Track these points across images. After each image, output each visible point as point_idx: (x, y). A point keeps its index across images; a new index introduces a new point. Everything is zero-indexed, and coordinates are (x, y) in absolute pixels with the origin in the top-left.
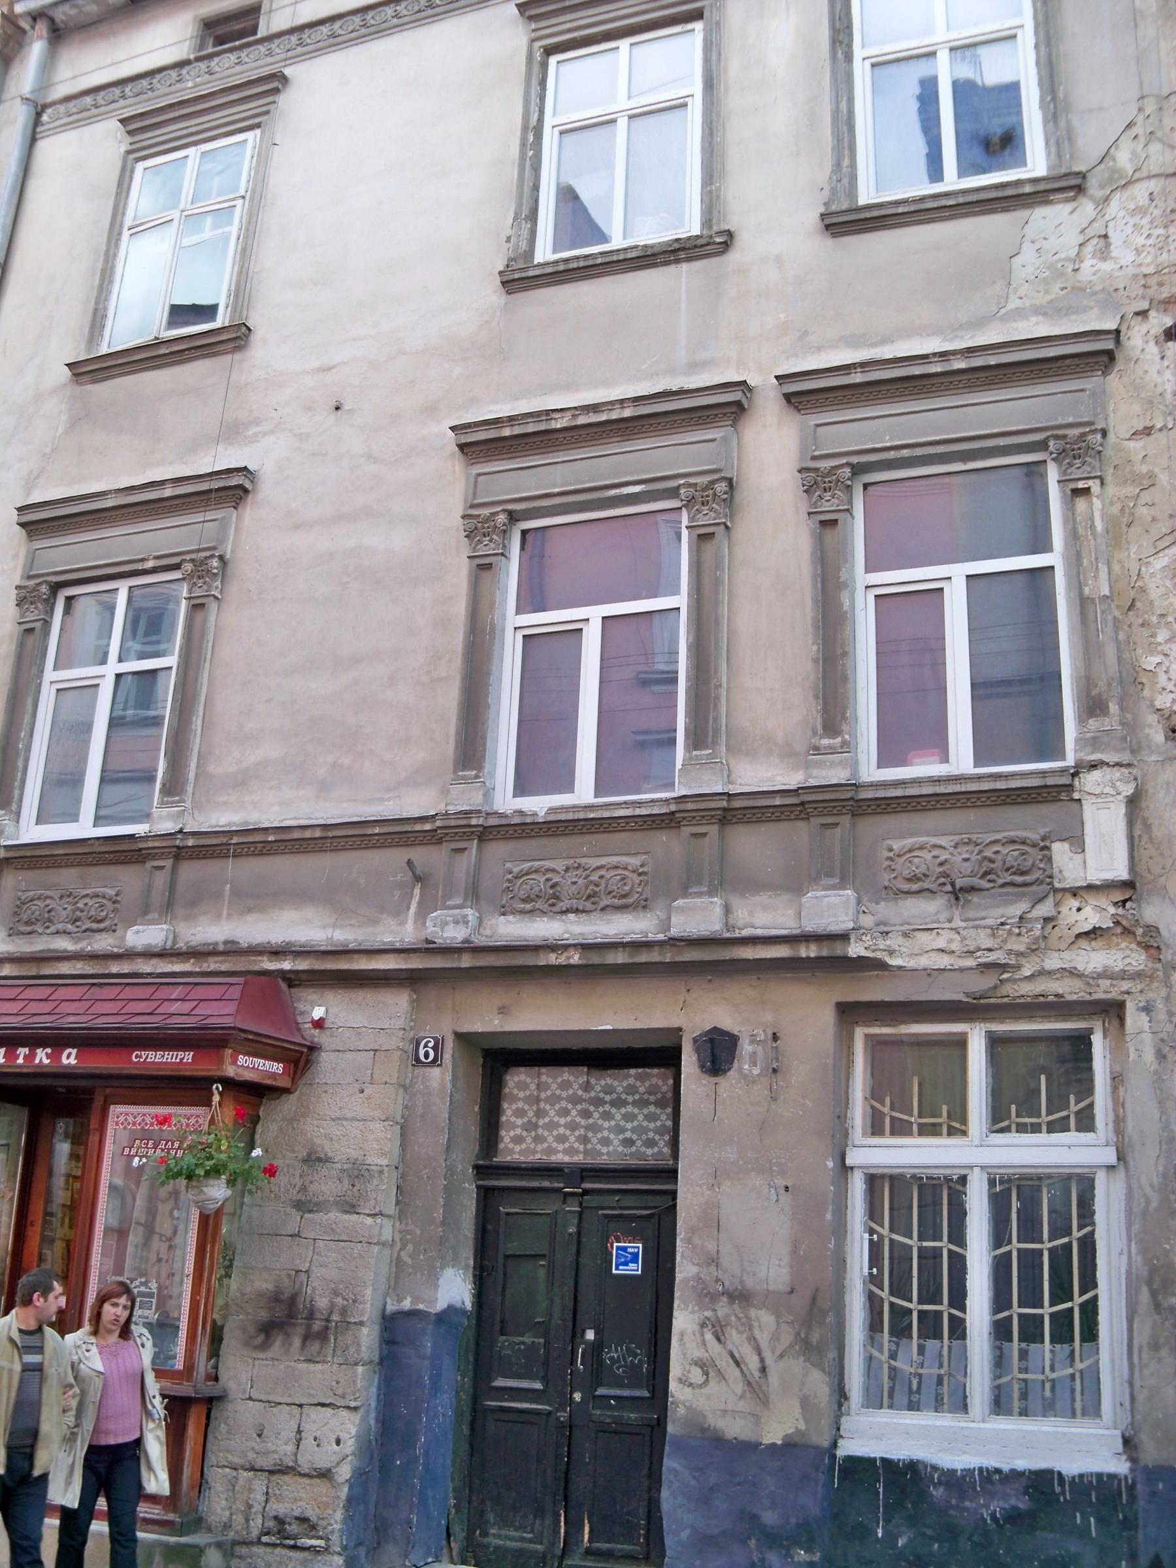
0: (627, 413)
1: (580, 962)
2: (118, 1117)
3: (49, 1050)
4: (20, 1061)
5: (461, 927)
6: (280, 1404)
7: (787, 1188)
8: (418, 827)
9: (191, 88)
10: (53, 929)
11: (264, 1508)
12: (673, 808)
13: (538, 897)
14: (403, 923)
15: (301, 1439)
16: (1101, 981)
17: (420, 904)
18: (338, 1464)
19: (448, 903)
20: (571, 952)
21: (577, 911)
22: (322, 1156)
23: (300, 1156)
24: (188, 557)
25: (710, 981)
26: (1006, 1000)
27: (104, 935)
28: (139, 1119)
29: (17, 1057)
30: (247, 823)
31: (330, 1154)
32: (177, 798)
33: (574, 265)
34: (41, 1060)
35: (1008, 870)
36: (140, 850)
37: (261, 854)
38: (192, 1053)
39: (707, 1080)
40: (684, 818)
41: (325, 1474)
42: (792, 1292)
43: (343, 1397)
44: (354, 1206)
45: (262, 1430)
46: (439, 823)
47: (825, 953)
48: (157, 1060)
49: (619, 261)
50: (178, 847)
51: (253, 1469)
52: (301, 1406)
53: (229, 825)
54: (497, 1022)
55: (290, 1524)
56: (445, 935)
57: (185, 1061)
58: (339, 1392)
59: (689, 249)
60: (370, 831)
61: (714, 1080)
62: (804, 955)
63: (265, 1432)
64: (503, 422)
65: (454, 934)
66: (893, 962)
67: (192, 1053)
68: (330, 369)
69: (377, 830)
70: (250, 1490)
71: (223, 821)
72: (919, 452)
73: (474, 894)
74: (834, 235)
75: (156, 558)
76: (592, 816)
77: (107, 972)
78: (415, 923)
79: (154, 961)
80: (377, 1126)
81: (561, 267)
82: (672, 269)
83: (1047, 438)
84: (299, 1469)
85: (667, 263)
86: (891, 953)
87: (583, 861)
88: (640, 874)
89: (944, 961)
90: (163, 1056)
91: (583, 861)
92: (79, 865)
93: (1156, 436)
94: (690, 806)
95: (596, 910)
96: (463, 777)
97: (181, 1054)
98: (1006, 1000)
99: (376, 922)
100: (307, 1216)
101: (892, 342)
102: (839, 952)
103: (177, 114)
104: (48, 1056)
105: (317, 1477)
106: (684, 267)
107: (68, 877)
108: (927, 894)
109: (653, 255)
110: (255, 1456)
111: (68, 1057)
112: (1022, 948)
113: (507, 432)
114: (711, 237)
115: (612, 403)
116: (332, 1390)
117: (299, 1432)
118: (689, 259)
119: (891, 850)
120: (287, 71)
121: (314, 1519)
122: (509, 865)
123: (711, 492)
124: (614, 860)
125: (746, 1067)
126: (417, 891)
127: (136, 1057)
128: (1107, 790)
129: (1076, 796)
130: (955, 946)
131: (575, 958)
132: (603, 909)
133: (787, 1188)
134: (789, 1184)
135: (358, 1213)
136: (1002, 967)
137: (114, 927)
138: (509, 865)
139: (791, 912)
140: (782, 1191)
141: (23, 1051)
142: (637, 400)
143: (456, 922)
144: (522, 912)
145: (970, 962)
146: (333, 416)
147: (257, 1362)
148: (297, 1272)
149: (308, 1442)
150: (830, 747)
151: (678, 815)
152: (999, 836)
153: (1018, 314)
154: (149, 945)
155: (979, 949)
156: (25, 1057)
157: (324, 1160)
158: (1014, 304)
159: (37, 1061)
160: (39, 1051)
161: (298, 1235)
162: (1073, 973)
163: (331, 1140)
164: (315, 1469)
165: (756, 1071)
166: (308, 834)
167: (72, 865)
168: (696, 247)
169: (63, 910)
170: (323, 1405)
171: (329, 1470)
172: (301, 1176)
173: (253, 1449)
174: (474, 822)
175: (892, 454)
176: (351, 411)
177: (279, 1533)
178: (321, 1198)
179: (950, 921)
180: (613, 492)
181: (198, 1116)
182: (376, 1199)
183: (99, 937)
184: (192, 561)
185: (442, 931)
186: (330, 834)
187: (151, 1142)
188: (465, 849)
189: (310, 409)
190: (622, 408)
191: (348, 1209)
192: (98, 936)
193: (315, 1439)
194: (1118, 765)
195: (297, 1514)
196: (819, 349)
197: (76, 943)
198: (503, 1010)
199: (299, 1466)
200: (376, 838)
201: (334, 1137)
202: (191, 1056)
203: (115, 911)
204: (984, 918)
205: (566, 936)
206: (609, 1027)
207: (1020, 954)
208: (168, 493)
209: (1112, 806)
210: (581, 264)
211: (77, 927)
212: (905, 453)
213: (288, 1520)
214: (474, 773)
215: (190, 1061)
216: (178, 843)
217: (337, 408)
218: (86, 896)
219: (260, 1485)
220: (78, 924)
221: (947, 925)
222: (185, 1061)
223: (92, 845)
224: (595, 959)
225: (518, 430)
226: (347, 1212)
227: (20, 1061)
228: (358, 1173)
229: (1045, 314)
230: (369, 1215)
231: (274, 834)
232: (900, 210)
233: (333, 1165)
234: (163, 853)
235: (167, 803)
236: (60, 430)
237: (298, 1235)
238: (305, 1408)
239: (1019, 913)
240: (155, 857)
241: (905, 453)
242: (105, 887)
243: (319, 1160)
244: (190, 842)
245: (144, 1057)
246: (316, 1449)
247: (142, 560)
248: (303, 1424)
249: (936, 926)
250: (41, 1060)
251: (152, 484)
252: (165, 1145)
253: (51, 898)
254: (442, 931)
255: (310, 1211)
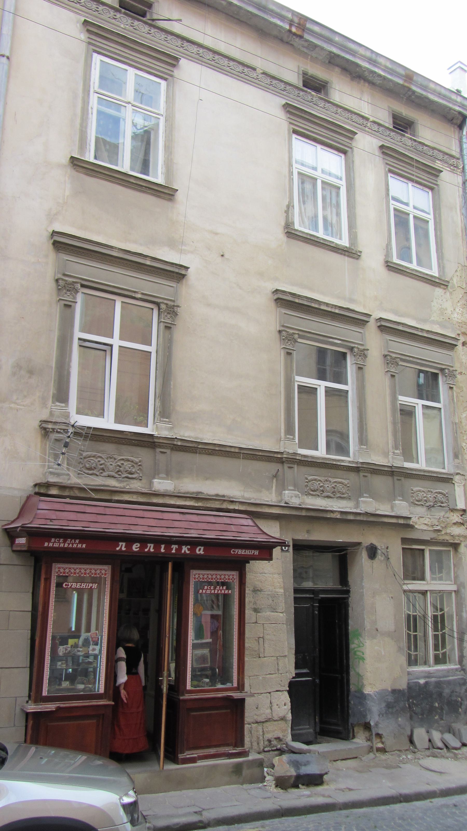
0: (337, 311)
1: (340, 518)
2: (195, 575)
3: (189, 547)
4: (174, 551)
5: (297, 499)
6: (262, 693)
7: (392, 597)
8: (276, 456)
9: (123, 28)
10: (105, 474)
11: (263, 737)
12: (360, 465)
13: (317, 490)
14: (271, 493)
15: (272, 706)
16: (456, 537)
17: (276, 486)
18: (287, 713)
19: (289, 488)
20: (337, 513)
21: (328, 497)
22: (259, 589)
23: (251, 589)
24: (165, 302)
25: (369, 527)
26: (436, 540)
27: (135, 481)
28: (214, 577)
29: (172, 549)
30: (198, 438)
31: (262, 588)
32: (168, 420)
33: (312, 238)
34: (185, 551)
35: (439, 502)
36: (154, 442)
37: (210, 454)
38: (258, 551)
39: (370, 561)
40: (362, 470)
41: (283, 719)
42: (395, 631)
43: (284, 686)
44: (275, 609)
45: (258, 706)
46: (285, 456)
47: (405, 523)
48: (242, 553)
49: (327, 245)
50: (174, 445)
51: (257, 722)
52: (270, 693)
53: (189, 437)
54: (306, 536)
55: (273, 741)
56: (292, 501)
57: (255, 554)
58: (283, 685)
59: (349, 252)
60: (258, 454)
61: (372, 561)
62: (400, 522)
63: (259, 706)
64: (296, 296)
65: (295, 502)
66: (416, 526)
67: (258, 551)
68: (216, 234)
69: (260, 454)
70: (257, 731)
71: (186, 434)
72: (415, 360)
73: (296, 486)
74: (389, 270)
75: (143, 294)
76: (334, 463)
77: (151, 501)
78: (276, 494)
79: (176, 498)
80: (276, 576)
81: (309, 237)
82: (342, 257)
83: (446, 368)
84: (274, 719)
85: (341, 254)
86: (416, 523)
87: (330, 479)
88: (348, 487)
89: (425, 528)
90: (245, 552)
91: (330, 479)
92: (116, 443)
93: (463, 375)
94: (365, 466)
95: (335, 497)
96: (288, 438)
97: (253, 551)
98: (436, 540)
99: (261, 492)
100: (258, 614)
101: (404, 317)
102: (408, 523)
103: (120, 41)
104: (188, 549)
105: (280, 720)
106: (346, 258)
107: (110, 448)
108: (421, 506)
109: (339, 249)
110: (257, 717)
111: (200, 550)
112: (443, 526)
113: (297, 301)
114: (356, 251)
115: (333, 305)
116: (280, 684)
117: (271, 703)
118: (348, 256)
119: (413, 490)
120: (183, 62)
121: (281, 737)
122: (306, 476)
123: (363, 353)
124: (340, 480)
125: (380, 557)
126: (275, 481)
127: (233, 551)
128: (460, 482)
129: (453, 482)
130: (429, 524)
131: (339, 516)
132: (337, 498)
133: (392, 597)
134: (392, 596)
135: (277, 612)
136: (439, 531)
137: (141, 478)
138: (306, 476)
139: (389, 507)
140: (391, 598)
141: (174, 547)
142: (341, 308)
143: (296, 497)
144: (312, 495)
145: (431, 529)
146: (220, 258)
147: (251, 677)
148: (259, 638)
149: (275, 707)
150: (397, 453)
151: (361, 468)
152: (437, 491)
153: (433, 322)
154: (167, 490)
155: (435, 525)
156: (176, 549)
157: (260, 591)
158: (432, 318)
159: (183, 552)
160: (184, 547)
161: (256, 622)
162: (450, 534)
163: (261, 582)
164: (279, 717)
165: (382, 559)
166: (233, 450)
167: (112, 442)
168: (352, 253)
169: (111, 465)
170: (277, 691)
171: (284, 717)
172: (253, 597)
173: (256, 715)
174: (298, 458)
175: (408, 358)
176: (228, 259)
177: (270, 745)
178: (263, 607)
179: (427, 515)
180: (331, 340)
181: (233, 575)
182: (282, 606)
183: (133, 482)
184: (167, 304)
185: (291, 499)
186: (242, 452)
187: (212, 587)
188: (292, 467)
189: (209, 249)
190: (332, 307)
191: (273, 610)
192: (132, 481)
193: (277, 705)
194: (462, 475)
195: (275, 737)
196: (385, 311)
197: (120, 483)
198: (308, 532)
199: (273, 717)
200: (259, 456)
201: (263, 581)
202: (257, 552)
203: (140, 469)
204: (435, 516)
205: (327, 506)
206: (341, 541)
207: (442, 528)
208: (148, 263)
209: (461, 487)
210: (316, 240)
211: (119, 475)
212: (411, 359)
213: (272, 740)
214: (292, 437)
215: (257, 554)
216: (175, 443)
217: (222, 256)
218: (123, 459)
219: (260, 728)
220: (120, 473)
221: (426, 516)
222: (255, 554)
223: (127, 435)
224: (345, 517)
225: (301, 302)
226: (273, 612)
227: (174, 551)
228: (274, 596)
229: (440, 325)
230: (280, 613)
231: (218, 447)
232: (407, 271)
233: (264, 593)
234: (166, 446)
235: (163, 421)
236: (67, 193)
237: (256, 622)
238: (272, 693)
239: (442, 515)
240: (160, 447)
241: (411, 359)
242: (132, 456)
243: (258, 590)
244: (179, 443)
245: (237, 552)
246: (279, 709)
247: (135, 292)
248: (272, 700)
249: (424, 516)
250: (185, 551)
251: (140, 255)
252: (219, 588)
253: (101, 457)
254: (291, 499)
255: (259, 612)
